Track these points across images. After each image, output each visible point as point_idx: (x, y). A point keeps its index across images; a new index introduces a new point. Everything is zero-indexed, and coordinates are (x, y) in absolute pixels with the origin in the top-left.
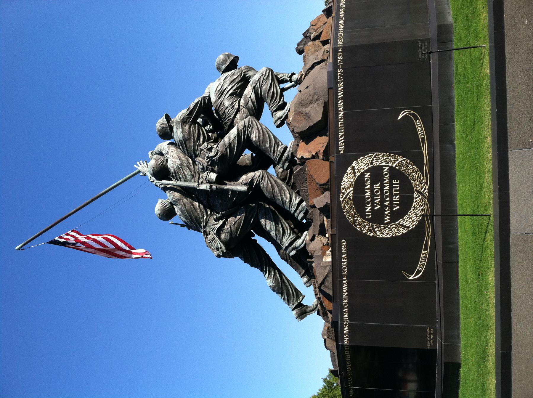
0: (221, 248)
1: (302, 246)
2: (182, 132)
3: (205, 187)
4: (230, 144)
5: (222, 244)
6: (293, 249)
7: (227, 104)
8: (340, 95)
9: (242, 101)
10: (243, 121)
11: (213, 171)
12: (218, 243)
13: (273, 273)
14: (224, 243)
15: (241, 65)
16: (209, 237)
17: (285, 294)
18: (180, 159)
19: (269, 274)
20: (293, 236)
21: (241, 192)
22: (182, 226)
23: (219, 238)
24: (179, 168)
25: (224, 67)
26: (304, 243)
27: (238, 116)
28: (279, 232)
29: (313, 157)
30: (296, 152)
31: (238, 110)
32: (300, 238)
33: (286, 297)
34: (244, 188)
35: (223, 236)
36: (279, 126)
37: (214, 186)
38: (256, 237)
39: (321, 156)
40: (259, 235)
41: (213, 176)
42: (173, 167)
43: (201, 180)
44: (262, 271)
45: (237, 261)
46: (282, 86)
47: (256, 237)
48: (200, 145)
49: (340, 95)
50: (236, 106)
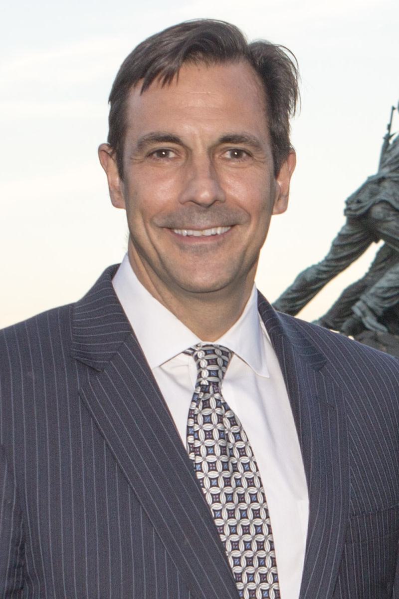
0: (362, 207)
1: (367, 326)
5: (366, 208)
6: (363, 313)
12: (367, 204)
13: (324, 276)
14: (368, 212)
16: (374, 186)
17: (295, 295)
19: (325, 272)
20: (380, 312)
22: (389, 127)
23: (374, 204)
26: (374, 329)
28: (386, 292)
33: (291, 296)
40: (379, 254)
44: (327, 260)
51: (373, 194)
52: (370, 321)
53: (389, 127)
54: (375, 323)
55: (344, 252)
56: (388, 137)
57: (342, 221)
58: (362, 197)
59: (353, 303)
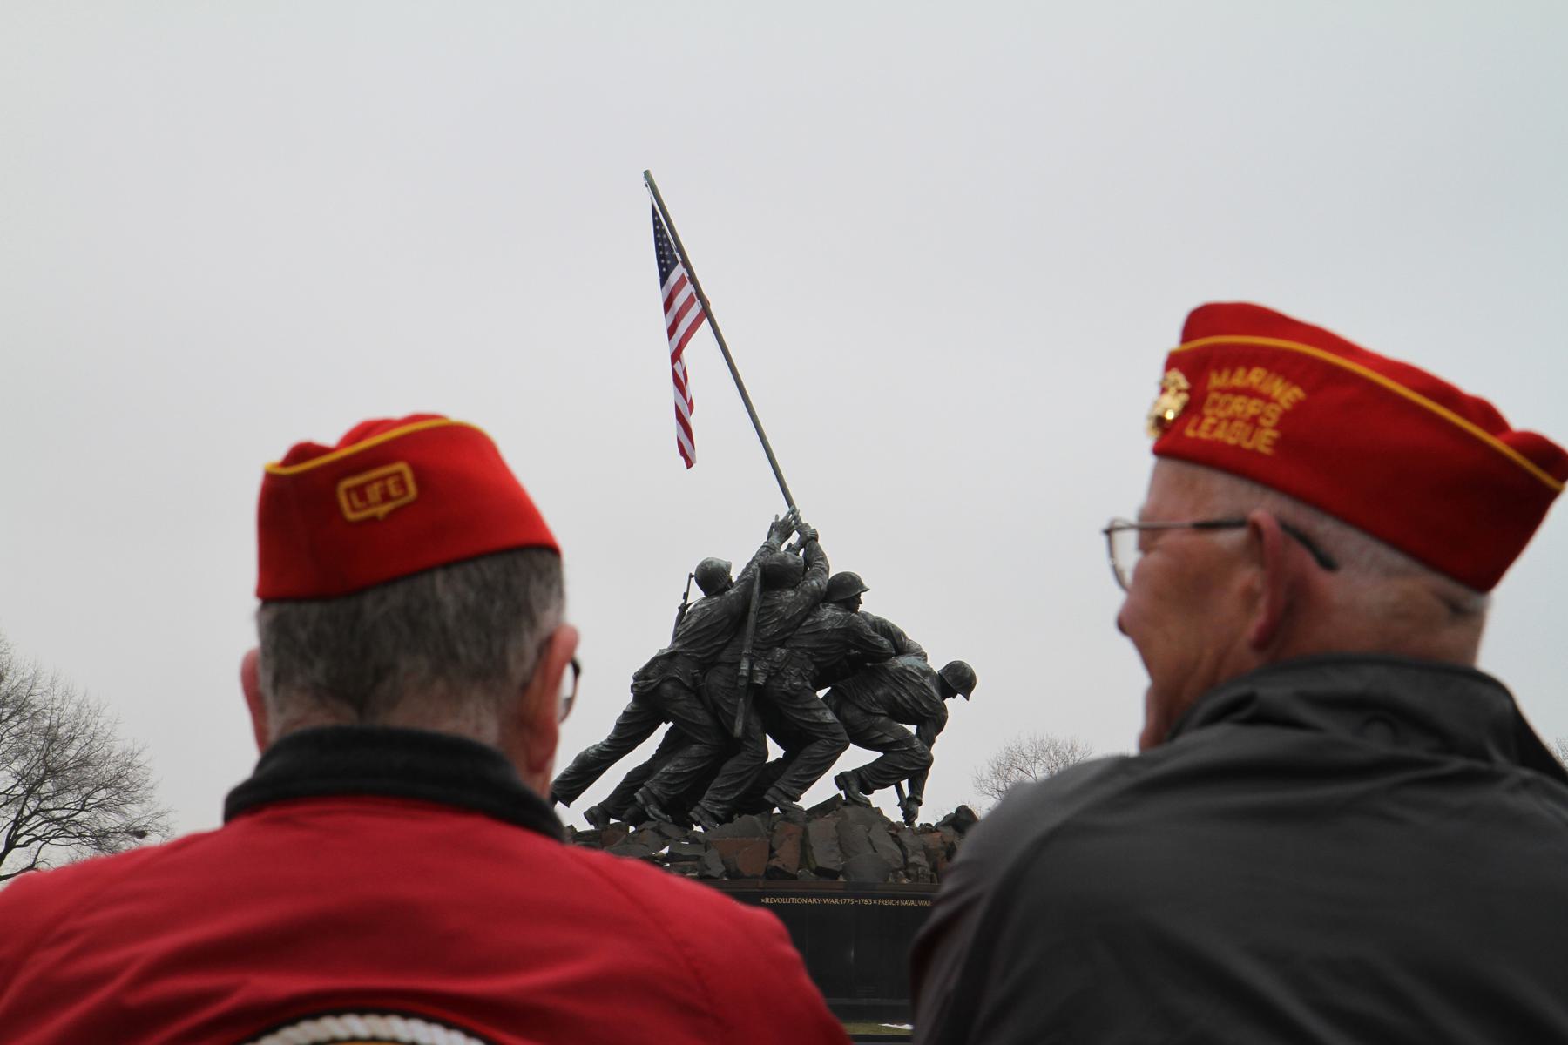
2: (833, 630)
3: (745, 666)
4: (808, 710)
7: (880, 692)
8: (826, 901)
9: (883, 719)
10: (843, 730)
11: (769, 677)
15: (953, 704)
18: (793, 618)
21: (733, 728)
22: (686, 596)
24: (779, 613)
25: (948, 679)
27: (858, 712)
29: (772, 850)
30: (787, 819)
31: (868, 713)
32: (664, 810)
34: (738, 729)
35: (668, 687)
36: (837, 779)
37: (742, 683)
38: (664, 728)
39: (774, 862)
41: (760, 680)
42: (781, 603)
43: (757, 653)
45: (625, 699)
46: (905, 784)
47: (664, 728)
48: (810, 657)
49: (826, 901)
50: (874, 709)
51: (663, 670)
52: (653, 810)
53: (686, 596)
54: (658, 812)
55: (628, 733)
56: (683, 608)
57: (630, 697)
58: (651, 673)
59: (636, 789)
